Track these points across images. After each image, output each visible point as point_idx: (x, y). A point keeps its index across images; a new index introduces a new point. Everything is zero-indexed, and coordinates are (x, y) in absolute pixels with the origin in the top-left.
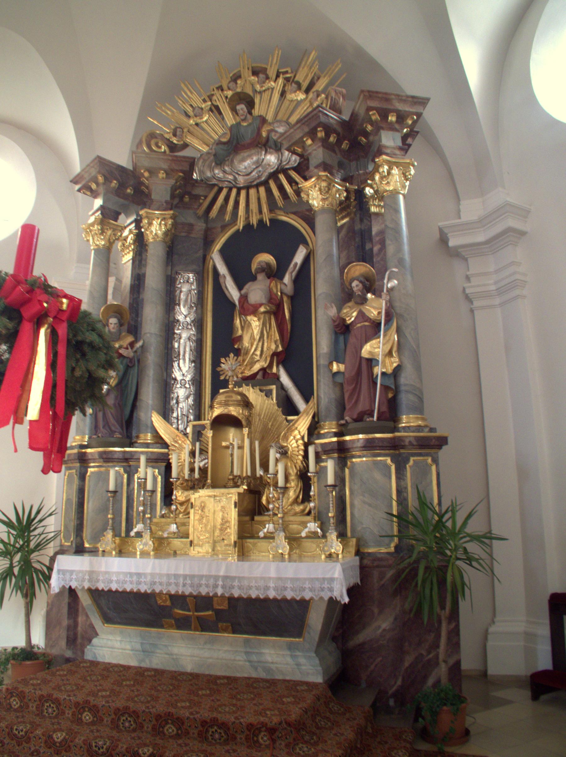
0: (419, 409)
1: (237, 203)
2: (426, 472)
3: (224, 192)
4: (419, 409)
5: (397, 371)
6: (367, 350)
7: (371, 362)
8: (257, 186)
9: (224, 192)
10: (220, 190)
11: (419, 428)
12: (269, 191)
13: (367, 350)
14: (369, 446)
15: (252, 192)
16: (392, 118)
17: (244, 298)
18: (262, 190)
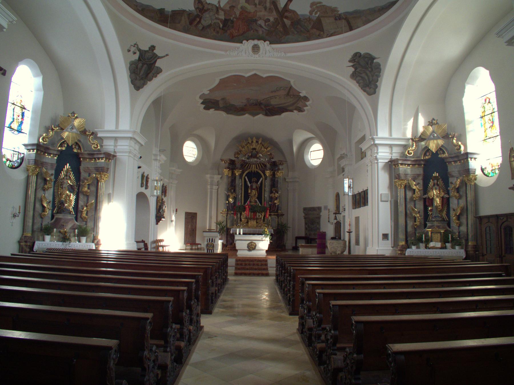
0: (281, 210)
1: (250, 166)
2: (281, 219)
3: (247, 165)
4: (281, 210)
5: (278, 205)
6: (275, 202)
7: (276, 203)
8: (254, 164)
9: (247, 165)
10: (247, 164)
11: (281, 213)
12: (256, 166)
13: (275, 202)
14: (274, 215)
15: (253, 165)
16: (282, 163)
17: (252, 186)
18: (255, 165)
